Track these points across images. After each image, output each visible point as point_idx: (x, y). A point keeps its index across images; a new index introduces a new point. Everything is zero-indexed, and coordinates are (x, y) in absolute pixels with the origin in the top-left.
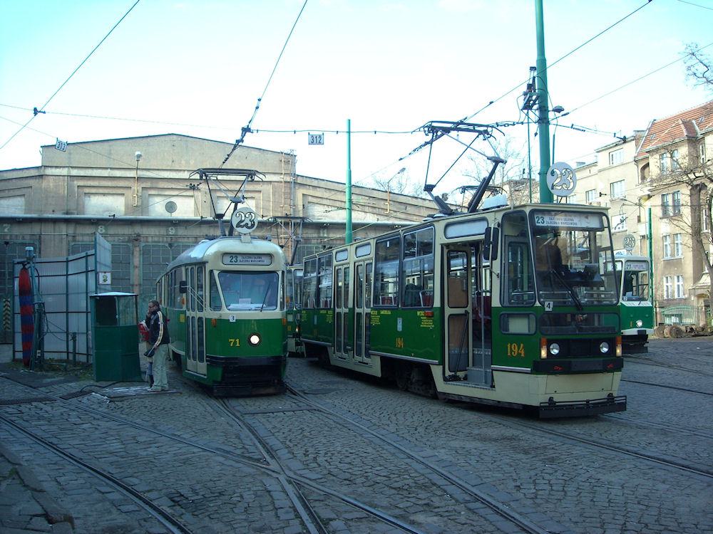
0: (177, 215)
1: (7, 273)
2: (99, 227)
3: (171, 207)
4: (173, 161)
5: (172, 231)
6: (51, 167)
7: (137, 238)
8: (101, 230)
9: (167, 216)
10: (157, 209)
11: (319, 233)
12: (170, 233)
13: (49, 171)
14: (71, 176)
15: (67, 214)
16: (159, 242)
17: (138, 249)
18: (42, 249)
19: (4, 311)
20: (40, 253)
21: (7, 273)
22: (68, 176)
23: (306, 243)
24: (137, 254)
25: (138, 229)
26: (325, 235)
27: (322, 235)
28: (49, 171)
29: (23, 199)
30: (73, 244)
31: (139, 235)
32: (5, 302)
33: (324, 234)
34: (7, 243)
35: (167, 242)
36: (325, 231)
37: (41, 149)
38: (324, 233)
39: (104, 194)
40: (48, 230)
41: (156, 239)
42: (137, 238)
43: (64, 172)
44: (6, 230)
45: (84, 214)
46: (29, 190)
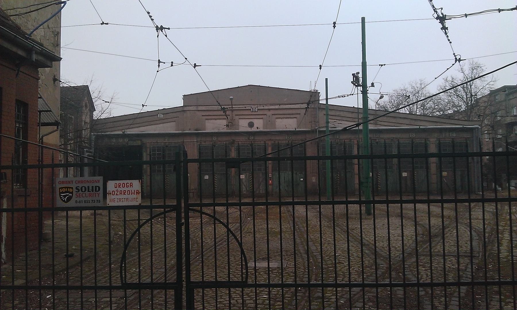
0: (254, 129)
3: (251, 125)
4: (251, 100)
5: (252, 138)
7: (233, 142)
8: (215, 139)
9: (249, 130)
10: (243, 126)
12: (251, 139)
16: (245, 144)
17: (234, 148)
24: (233, 150)
25: (233, 138)
26: (338, 137)
27: (335, 137)
28: (185, 109)
29: (174, 123)
31: (234, 141)
34: (167, 146)
35: (249, 143)
39: (216, 119)
40: (187, 140)
41: (244, 142)
42: (233, 142)
43: (194, 108)
44: (166, 140)
45: (205, 131)
46: (177, 118)
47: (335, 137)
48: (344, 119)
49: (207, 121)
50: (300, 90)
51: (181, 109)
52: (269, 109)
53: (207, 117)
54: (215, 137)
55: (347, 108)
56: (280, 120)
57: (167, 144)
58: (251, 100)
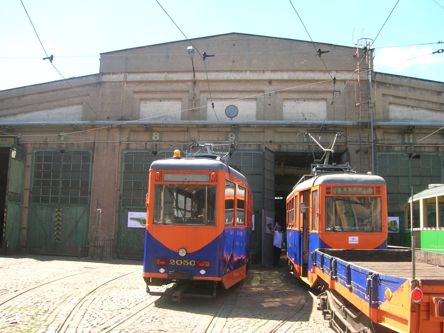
1: (61, 182)
2: (154, 134)
4: (233, 62)
6: (109, 74)
11: (403, 139)
13: (106, 78)
14: (127, 82)
15: (122, 119)
18: (94, 157)
19: (56, 221)
20: (93, 161)
21: (61, 182)
22: (124, 82)
23: (388, 151)
26: (411, 141)
27: (406, 141)
28: (106, 78)
30: (126, 152)
32: (57, 212)
33: (409, 139)
34: (63, 152)
36: (411, 136)
37: (100, 55)
38: (409, 139)
43: (121, 77)
47: (406, 141)
48: (424, 104)
49: (143, 104)
50: (334, 44)
51: (94, 80)
52: (270, 82)
53: (144, 96)
54: (156, 134)
55: (428, 83)
56: (292, 103)
57: (64, 146)
58: (233, 62)
